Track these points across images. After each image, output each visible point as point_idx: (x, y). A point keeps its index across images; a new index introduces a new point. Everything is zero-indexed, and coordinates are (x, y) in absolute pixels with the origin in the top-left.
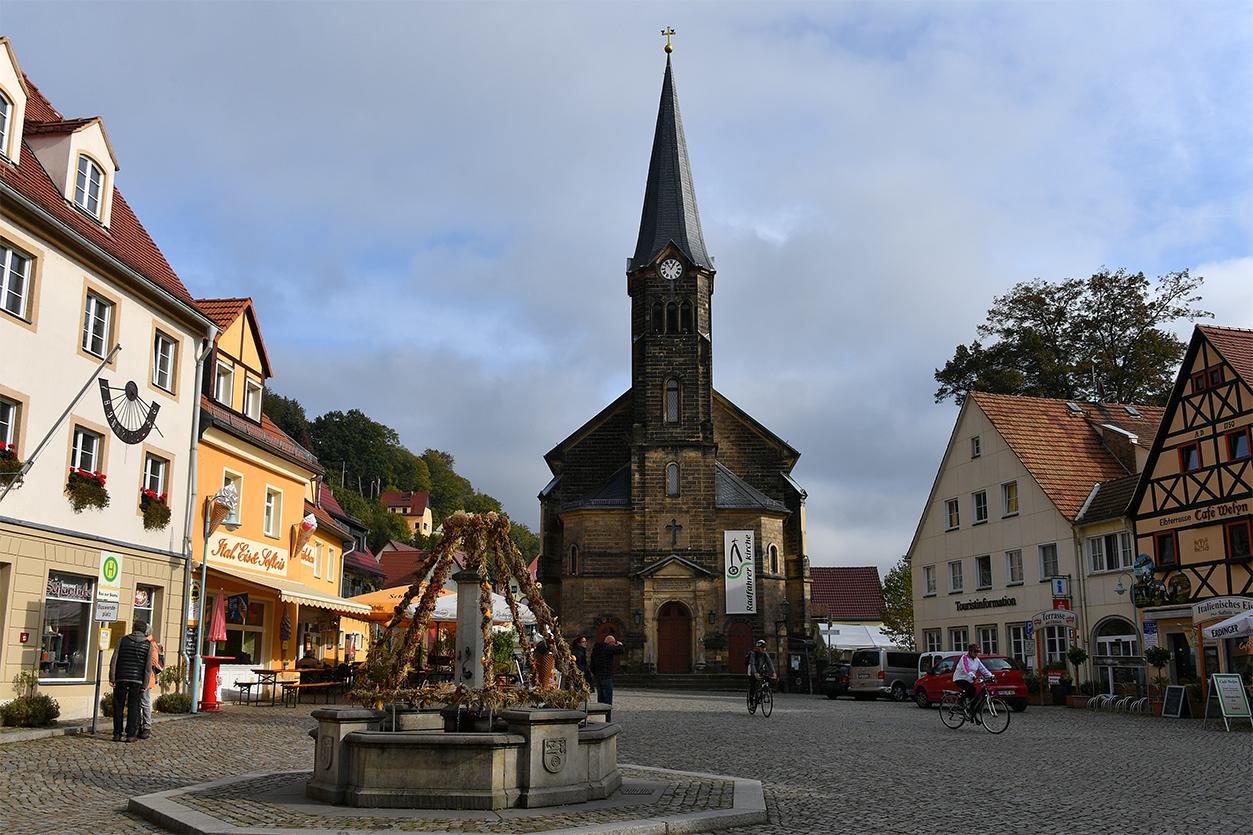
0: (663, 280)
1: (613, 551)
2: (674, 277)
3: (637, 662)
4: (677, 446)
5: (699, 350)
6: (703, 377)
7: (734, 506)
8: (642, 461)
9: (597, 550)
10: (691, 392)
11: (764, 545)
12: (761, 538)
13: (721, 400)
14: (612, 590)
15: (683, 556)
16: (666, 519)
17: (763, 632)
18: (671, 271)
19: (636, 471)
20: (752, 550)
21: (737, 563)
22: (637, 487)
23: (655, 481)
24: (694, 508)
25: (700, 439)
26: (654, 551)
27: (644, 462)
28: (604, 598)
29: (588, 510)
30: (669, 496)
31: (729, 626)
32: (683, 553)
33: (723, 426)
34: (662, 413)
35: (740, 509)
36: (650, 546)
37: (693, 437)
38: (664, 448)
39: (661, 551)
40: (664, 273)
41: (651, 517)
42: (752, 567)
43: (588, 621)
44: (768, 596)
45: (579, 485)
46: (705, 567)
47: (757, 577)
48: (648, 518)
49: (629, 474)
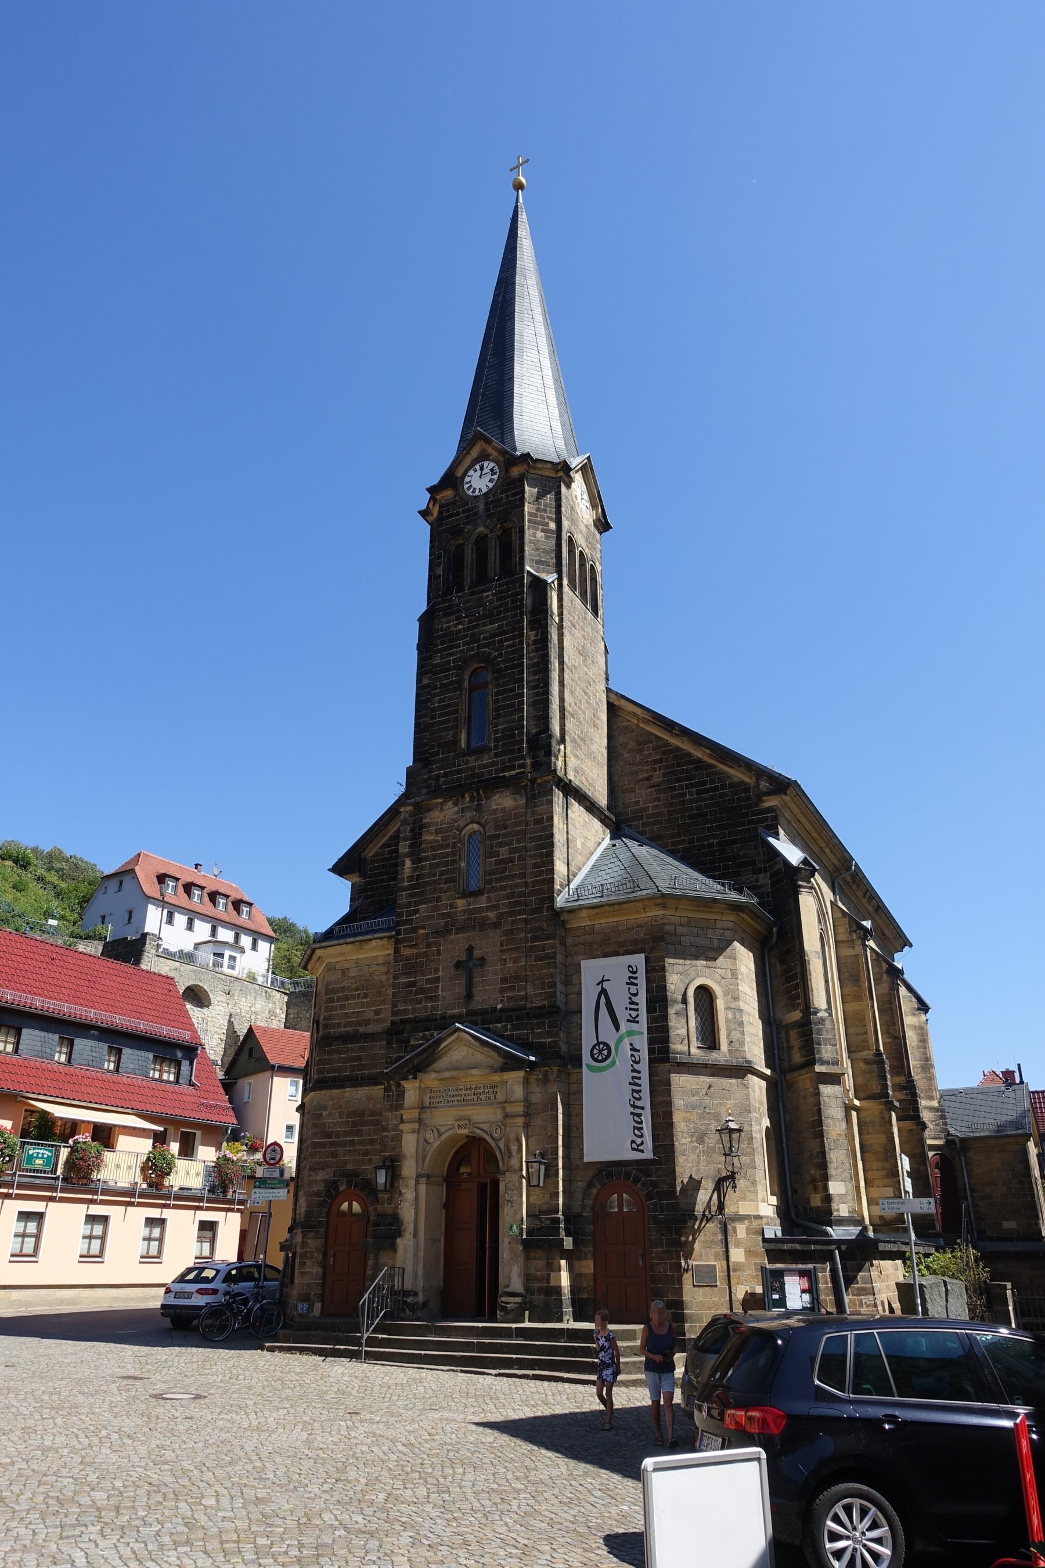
2: (485, 490)
14: (361, 1114)
16: (454, 947)
19: (407, 855)
20: (642, 999)
22: (405, 889)
24: (511, 913)
26: (429, 1019)
27: (420, 835)
28: (346, 1134)
31: (595, 1191)
37: (512, 768)
41: (429, 945)
44: (691, 1108)
47: (652, 1061)
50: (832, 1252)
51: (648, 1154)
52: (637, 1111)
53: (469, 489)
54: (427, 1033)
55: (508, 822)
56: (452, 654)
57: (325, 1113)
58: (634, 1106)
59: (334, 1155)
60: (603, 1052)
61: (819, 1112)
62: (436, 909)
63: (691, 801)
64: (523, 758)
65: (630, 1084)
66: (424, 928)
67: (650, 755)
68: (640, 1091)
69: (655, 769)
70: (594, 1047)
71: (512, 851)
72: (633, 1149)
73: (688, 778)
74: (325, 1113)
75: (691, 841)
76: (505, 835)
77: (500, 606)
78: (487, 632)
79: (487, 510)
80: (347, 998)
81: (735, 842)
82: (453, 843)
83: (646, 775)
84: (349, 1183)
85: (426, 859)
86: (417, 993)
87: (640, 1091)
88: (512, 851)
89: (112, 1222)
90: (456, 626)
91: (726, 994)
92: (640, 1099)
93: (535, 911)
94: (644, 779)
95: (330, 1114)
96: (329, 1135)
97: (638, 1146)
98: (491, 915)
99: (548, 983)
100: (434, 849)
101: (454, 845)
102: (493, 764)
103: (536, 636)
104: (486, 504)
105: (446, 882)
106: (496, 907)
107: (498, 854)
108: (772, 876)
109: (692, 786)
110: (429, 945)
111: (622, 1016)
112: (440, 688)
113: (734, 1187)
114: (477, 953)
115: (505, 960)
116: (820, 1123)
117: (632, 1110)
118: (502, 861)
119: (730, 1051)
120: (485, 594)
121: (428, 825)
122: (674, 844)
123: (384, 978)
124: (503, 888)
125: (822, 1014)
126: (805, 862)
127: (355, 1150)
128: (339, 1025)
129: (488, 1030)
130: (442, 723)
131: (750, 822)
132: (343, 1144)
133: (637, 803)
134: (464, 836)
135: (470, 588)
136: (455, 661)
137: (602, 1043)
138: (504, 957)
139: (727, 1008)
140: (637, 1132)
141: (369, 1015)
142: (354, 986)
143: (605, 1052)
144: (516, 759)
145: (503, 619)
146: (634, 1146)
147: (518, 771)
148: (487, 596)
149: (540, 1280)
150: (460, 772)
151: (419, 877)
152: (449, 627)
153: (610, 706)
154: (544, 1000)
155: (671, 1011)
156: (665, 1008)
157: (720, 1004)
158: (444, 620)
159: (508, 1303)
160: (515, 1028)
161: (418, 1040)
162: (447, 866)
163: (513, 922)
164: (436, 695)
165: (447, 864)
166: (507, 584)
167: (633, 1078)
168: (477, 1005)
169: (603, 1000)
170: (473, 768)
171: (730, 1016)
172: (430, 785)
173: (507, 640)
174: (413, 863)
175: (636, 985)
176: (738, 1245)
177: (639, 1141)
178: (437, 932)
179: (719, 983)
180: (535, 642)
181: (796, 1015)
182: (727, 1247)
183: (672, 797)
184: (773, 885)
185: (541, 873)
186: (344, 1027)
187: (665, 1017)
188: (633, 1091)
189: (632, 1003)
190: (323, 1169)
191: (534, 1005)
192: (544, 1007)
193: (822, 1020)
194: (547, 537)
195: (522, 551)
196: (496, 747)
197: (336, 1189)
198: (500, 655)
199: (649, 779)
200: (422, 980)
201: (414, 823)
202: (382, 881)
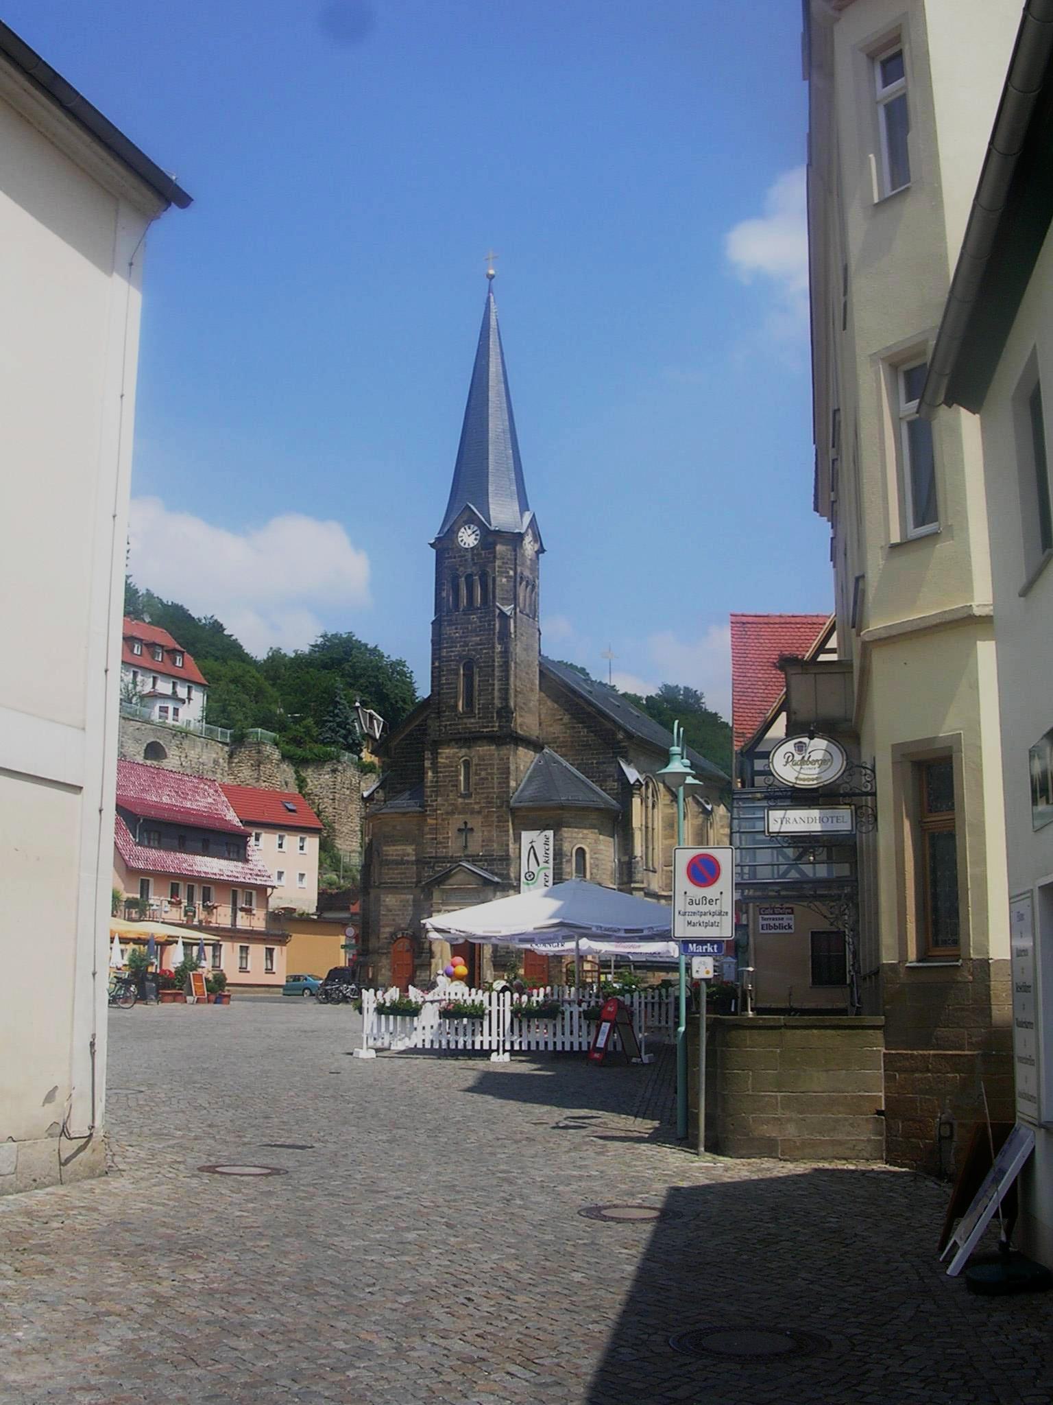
0: (460, 549)
2: (472, 545)
3: (425, 980)
4: (469, 739)
5: (497, 625)
6: (501, 657)
9: (394, 857)
10: (485, 676)
11: (569, 848)
12: (561, 840)
15: (474, 862)
16: (457, 821)
18: (468, 538)
20: (551, 852)
21: (534, 867)
24: (488, 807)
27: (437, 758)
29: (383, 814)
32: (474, 859)
36: (442, 852)
37: (487, 727)
38: (457, 741)
39: (452, 857)
40: (465, 544)
41: (443, 820)
43: (385, 936)
46: (496, 874)
48: (440, 821)
49: (422, 772)
50: (630, 966)
56: (452, 651)
60: (531, 876)
62: (447, 800)
64: (493, 722)
66: (440, 810)
75: (582, 760)
76: (483, 765)
79: (473, 559)
81: (604, 763)
84: (403, 933)
85: (441, 772)
89: (250, 951)
90: (455, 633)
91: (591, 851)
93: (498, 807)
94: (559, 720)
98: (476, 807)
100: (444, 767)
102: (477, 723)
104: (473, 555)
105: (453, 786)
106: (479, 803)
107: (480, 774)
110: (443, 820)
111: (541, 860)
114: (469, 826)
118: (482, 779)
119: (591, 878)
122: (573, 760)
124: (482, 793)
126: (638, 780)
128: (392, 855)
130: (448, 693)
135: (463, 610)
136: (455, 656)
139: (591, 858)
144: (490, 722)
145: (483, 635)
150: (459, 724)
151: (437, 782)
156: (561, 859)
157: (588, 856)
158: (448, 628)
160: (488, 865)
164: (444, 675)
165: (452, 776)
168: (469, 852)
169: (532, 850)
170: (466, 724)
173: (485, 649)
179: (588, 846)
180: (501, 652)
181: (625, 859)
185: (502, 788)
187: (561, 863)
192: (502, 856)
193: (638, 862)
194: (508, 581)
195: (494, 593)
196: (479, 713)
197: (396, 936)
199: (561, 719)
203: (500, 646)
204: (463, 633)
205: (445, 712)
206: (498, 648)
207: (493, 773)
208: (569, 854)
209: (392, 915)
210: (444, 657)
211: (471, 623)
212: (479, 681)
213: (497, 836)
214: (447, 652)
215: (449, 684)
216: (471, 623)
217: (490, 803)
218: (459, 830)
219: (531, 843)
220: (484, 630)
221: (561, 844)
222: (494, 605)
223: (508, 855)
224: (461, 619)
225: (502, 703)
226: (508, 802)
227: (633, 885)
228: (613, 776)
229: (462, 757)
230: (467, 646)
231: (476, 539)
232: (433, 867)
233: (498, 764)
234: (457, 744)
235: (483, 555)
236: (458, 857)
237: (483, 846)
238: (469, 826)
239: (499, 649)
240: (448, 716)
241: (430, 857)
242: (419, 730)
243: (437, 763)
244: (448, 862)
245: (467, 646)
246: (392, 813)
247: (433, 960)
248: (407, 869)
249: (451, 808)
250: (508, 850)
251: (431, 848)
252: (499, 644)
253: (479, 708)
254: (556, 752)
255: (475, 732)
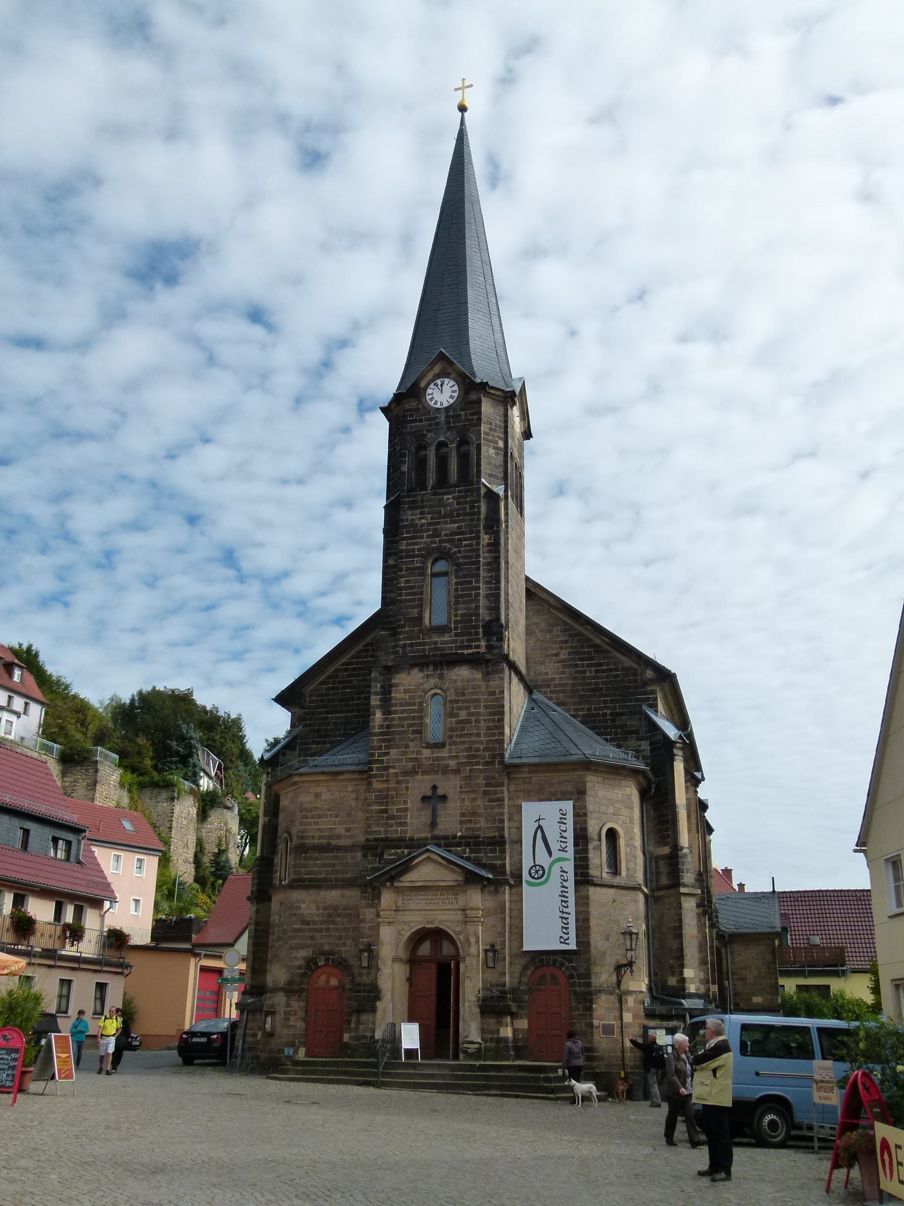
0: (428, 410)
1: (342, 842)
2: (446, 404)
3: (364, 1037)
7: (537, 760)
8: (387, 691)
9: (317, 841)
10: (465, 576)
11: (593, 827)
12: (585, 815)
13: (544, 596)
14: (336, 908)
16: (420, 785)
17: (589, 985)
19: (377, 707)
20: (570, 835)
21: (543, 858)
23: (406, 723)
24: (469, 763)
25: (483, 650)
28: (321, 922)
29: (301, 775)
30: (429, 746)
31: (529, 972)
32: (448, 842)
33: (548, 637)
34: (421, 613)
35: (548, 765)
36: (396, 831)
37: (470, 647)
39: (412, 839)
42: (570, 867)
45: (325, 743)
47: (577, 883)
49: (366, 713)
51: (573, 946)
52: (565, 915)
53: (431, 399)
54: (398, 850)
55: (466, 691)
56: (416, 544)
57: (303, 906)
58: (563, 912)
59: (312, 938)
60: (539, 873)
61: (680, 921)
62: (404, 754)
63: (591, 678)
64: (478, 640)
65: (560, 896)
66: (394, 767)
67: (558, 636)
68: (567, 901)
69: (562, 648)
70: (531, 868)
71: (470, 714)
72: (561, 942)
73: (589, 659)
74: (303, 906)
75: (589, 709)
77: (459, 509)
78: (448, 529)
79: (448, 423)
80: (320, 816)
81: (623, 714)
82: (419, 702)
83: (554, 652)
84: (327, 960)
85: (396, 712)
86: (387, 818)
87: (567, 901)
88: (470, 714)
89: (74, 986)
90: (420, 519)
92: (567, 907)
95: (307, 907)
96: (308, 923)
97: (565, 940)
99: (499, 820)
100: (402, 705)
101: (421, 704)
103: (490, 539)
104: (447, 417)
105: (414, 732)
106: (456, 757)
107: (457, 715)
108: (651, 745)
109: (592, 665)
110: (399, 782)
111: (555, 846)
112: (406, 571)
113: (632, 971)
114: (440, 792)
115: (464, 799)
116: (680, 928)
117: (561, 915)
120: (446, 497)
121: (397, 685)
122: (575, 710)
123: (353, 803)
125: (685, 851)
127: (330, 936)
128: (313, 837)
129: (450, 851)
130: (409, 601)
131: (637, 700)
132: (321, 930)
133: (547, 673)
134: (428, 698)
135: (433, 488)
136: (419, 550)
137: (538, 865)
138: (463, 797)
139: (627, 845)
140: (564, 930)
141: (340, 830)
142: (326, 807)
143: (541, 872)
144: (472, 641)
145: (462, 521)
146: (562, 940)
147: (475, 650)
148: (448, 499)
149: (492, 1032)
150: (424, 644)
151: (388, 727)
152: (414, 520)
153: (528, 590)
154: (495, 832)
155: (591, 846)
156: (587, 843)
157: (622, 842)
158: (409, 512)
159: (469, 1048)
160: (472, 851)
161: (390, 855)
162: (414, 720)
163: (471, 770)
164: (403, 576)
165: (414, 718)
166: (466, 491)
167: (562, 892)
169: (539, 833)
170: (436, 643)
171: (628, 850)
172: (396, 653)
173: (466, 539)
174: (384, 714)
175: (566, 824)
176: (628, 1010)
177: (565, 937)
178: (405, 772)
179: (621, 826)
180: (489, 545)
181: (666, 850)
182: (621, 1011)
183: (576, 672)
184: (651, 751)
185: (494, 735)
186: (318, 839)
187: (586, 851)
188: (562, 901)
189: (562, 837)
190: (304, 949)
191: (487, 835)
192: (495, 837)
193: (685, 855)
194: (497, 454)
195: (479, 465)
196: (456, 628)
197: (316, 964)
198: (460, 552)
199: (557, 655)
200: (393, 809)
201: (384, 681)
202: (320, 713)
203: (487, 536)
204: (432, 518)
205: (404, 626)
206: (485, 539)
207: (478, 714)
208: (596, 837)
209: (311, 930)
210: (401, 551)
211: (445, 506)
212: (457, 584)
213: (486, 807)
214: (407, 545)
215: (411, 588)
216: (445, 506)
217: (474, 757)
218: (424, 799)
219: (539, 819)
220: (465, 514)
221: (585, 822)
222: (479, 481)
223: (503, 837)
224: (431, 500)
225: (490, 615)
226: (502, 756)
227: (682, 890)
228: (636, 732)
229: (432, 689)
230: (439, 535)
231: (451, 397)
232: (382, 855)
233: (486, 701)
234: (421, 671)
235: (463, 417)
236: (421, 839)
237: (461, 822)
238: (440, 792)
239: (487, 541)
240: (407, 632)
241: (376, 840)
242: (346, 670)
243: (390, 699)
244: (407, 847)
245: (439, 535)
246: (316, 773)
247: (378, 1003)
248: (336, 858)
249: (410, 765)
250: (503, 829)
251: (378, 825)
252: (486, 533)
253: (456, 622)
254: (550, 699)
255: (448, 654)
